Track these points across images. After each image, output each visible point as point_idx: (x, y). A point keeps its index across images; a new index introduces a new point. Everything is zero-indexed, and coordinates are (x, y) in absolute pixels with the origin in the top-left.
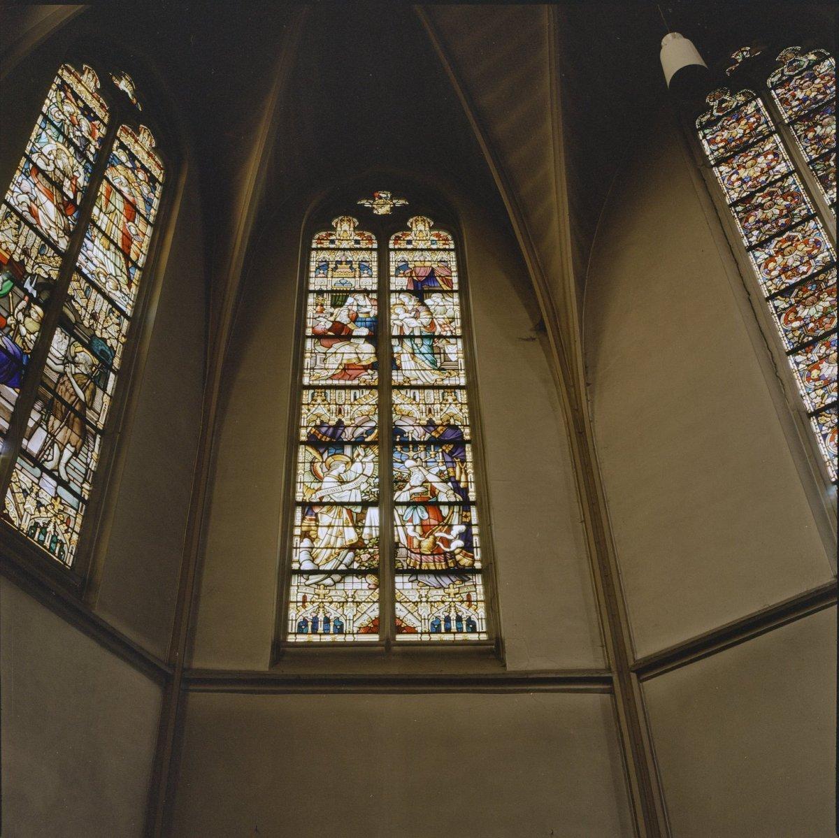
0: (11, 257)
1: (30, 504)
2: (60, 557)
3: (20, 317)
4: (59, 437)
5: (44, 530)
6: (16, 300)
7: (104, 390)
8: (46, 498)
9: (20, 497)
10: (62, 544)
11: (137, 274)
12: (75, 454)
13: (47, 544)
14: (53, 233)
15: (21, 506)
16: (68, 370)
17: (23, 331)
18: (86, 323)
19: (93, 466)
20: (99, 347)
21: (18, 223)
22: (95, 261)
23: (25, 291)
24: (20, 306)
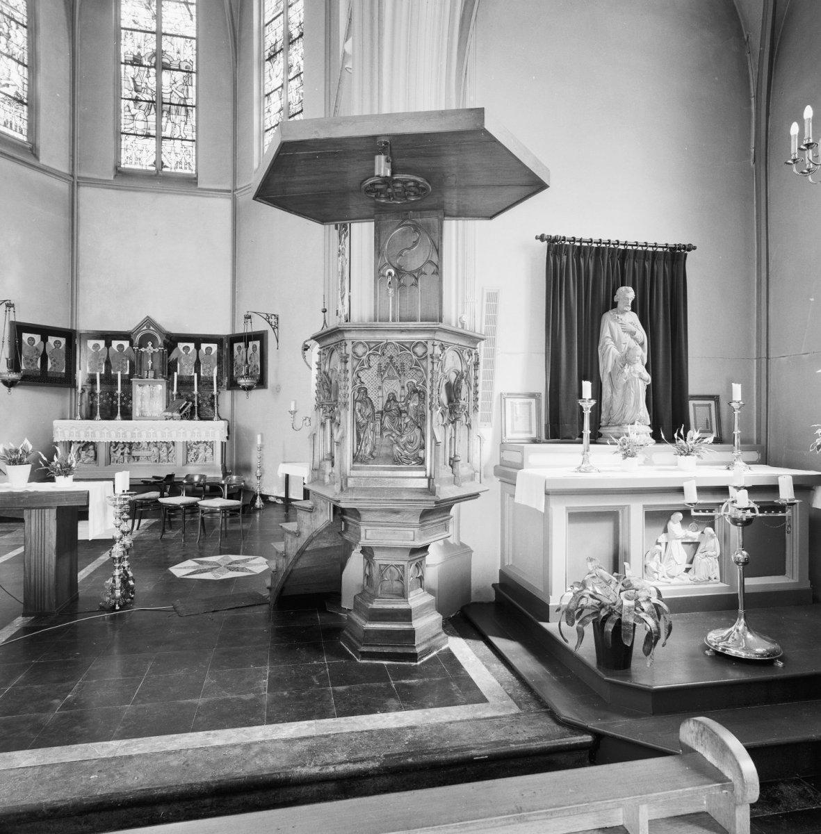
0: (134, 55)
1: (173, 155)
2: (190, 169)
3: (146, 80)
4: (177, 121)
5: (181, 163)
6: (142, 73)
7: (192, 85)
8: (178, 150)
9: (168, 156)
10: (189, 163)
11: (193, 8)
12: (186, 124)
13: (183, 167)
14: (148, 25)
15: (169, 160)
16: (173, 88)
17: (149, 86)
18: (175, 59)
19: (194, 124)
20: (183, 68)
21: (131, 34)
22: (172, 21)
23: (145, 66)
24: (145, 75)
